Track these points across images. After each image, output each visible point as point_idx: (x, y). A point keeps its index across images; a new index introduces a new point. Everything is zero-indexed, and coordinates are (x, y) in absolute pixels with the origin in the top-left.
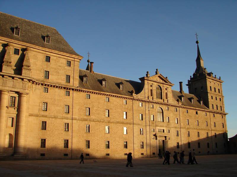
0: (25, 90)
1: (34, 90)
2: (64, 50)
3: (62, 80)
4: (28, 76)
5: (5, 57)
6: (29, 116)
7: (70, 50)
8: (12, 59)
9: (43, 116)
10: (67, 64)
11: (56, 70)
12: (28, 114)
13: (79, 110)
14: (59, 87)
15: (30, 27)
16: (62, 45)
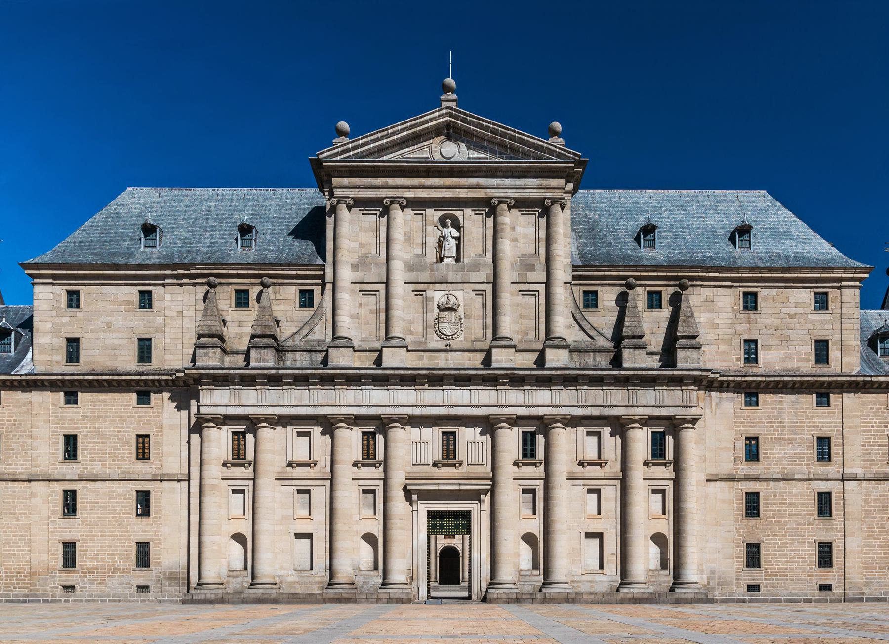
0: (691, 407)
1: (717, 404)
2: (804, 258)
3: (803, 360)
4: (696, 366)
5: (626, 324)
6: (708, 480)
7: (823, 254)
8: (644, 324)
9: (748, 478)
10: (816, 302)
11: (779, 332)
12: (703, 477)
13: (863, 446)
14: (794, 383)
15: (685, 210)
16: (794, 244)
